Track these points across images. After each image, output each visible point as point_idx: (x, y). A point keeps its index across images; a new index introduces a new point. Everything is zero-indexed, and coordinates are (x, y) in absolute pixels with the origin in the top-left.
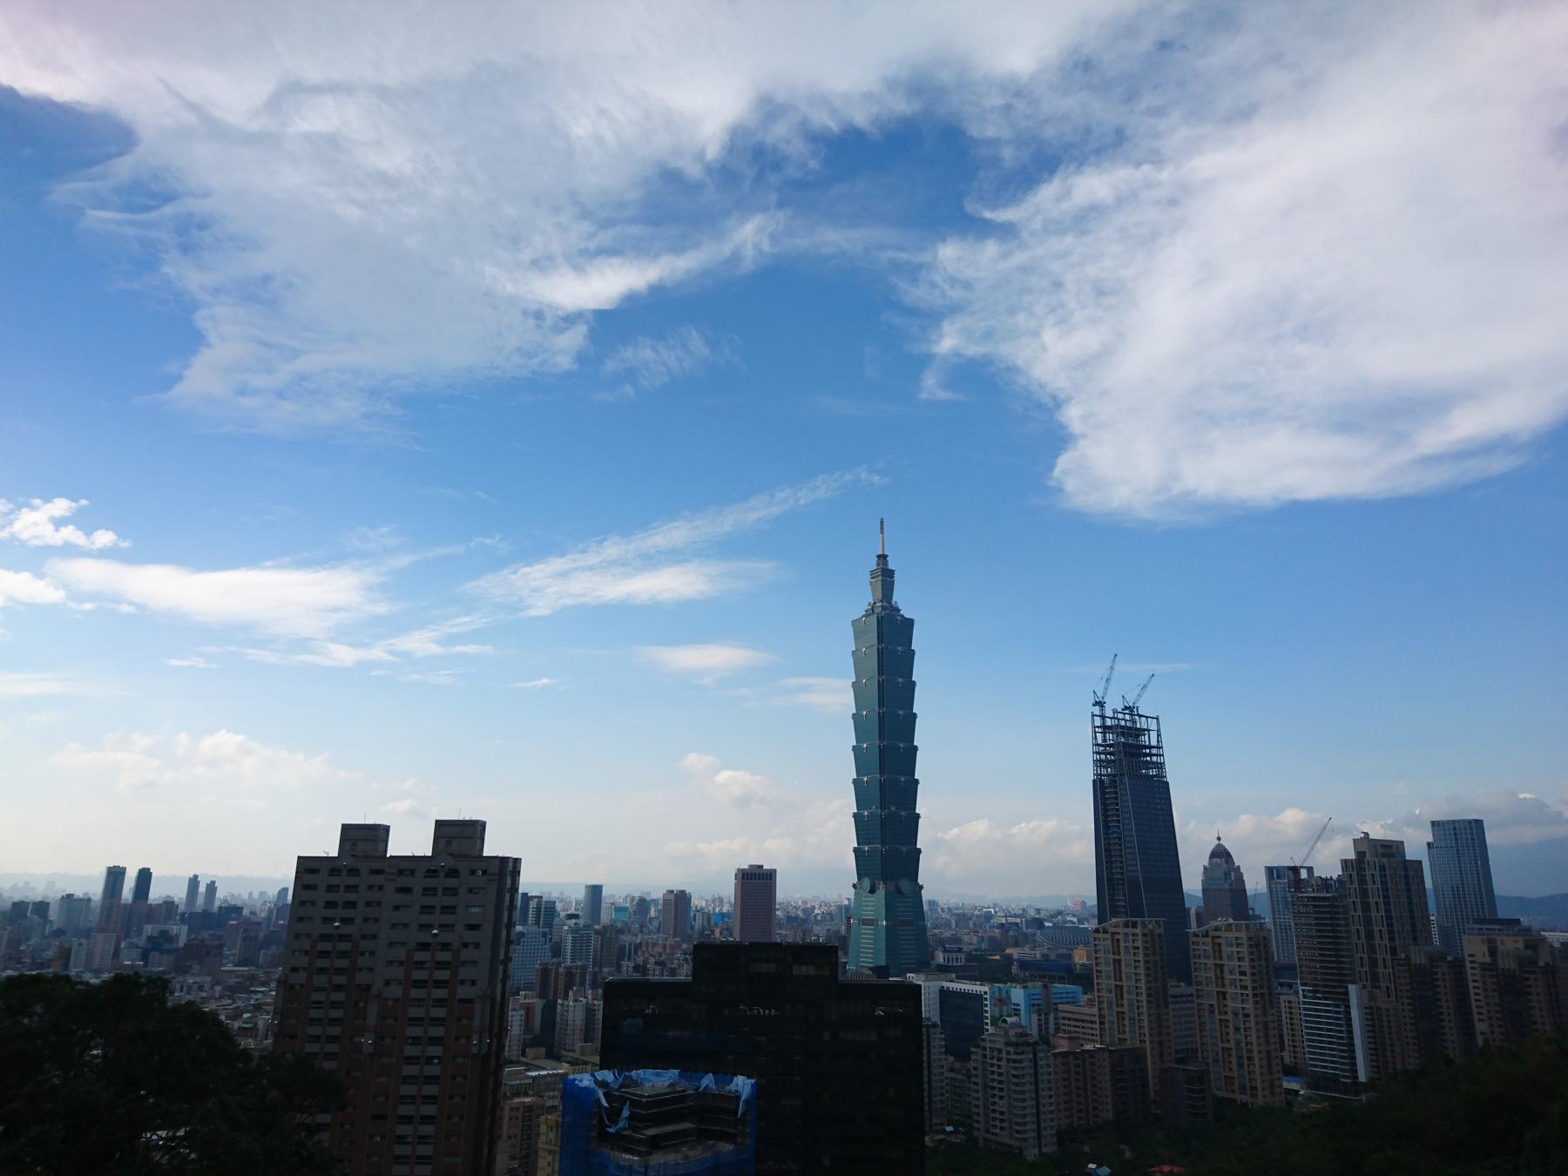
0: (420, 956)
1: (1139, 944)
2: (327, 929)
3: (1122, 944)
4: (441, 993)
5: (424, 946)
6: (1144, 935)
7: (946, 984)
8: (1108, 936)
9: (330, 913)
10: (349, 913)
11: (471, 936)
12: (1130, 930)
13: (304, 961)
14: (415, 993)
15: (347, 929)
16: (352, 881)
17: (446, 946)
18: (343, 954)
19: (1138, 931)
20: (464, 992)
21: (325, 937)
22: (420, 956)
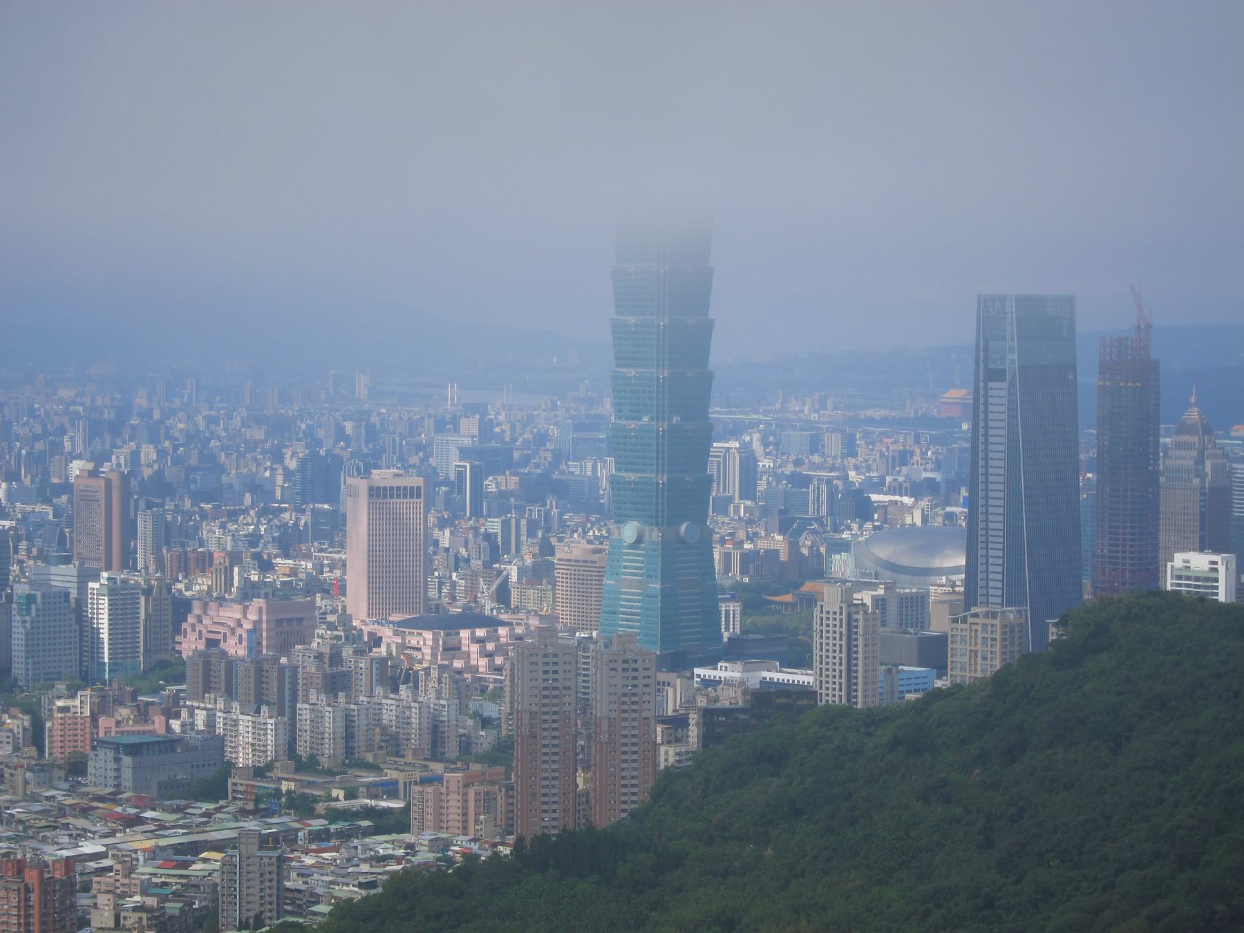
0: (624, 699)
1: (998, 636)
2: (546, 684)
3: (980, 634)
4: (636, 715)
5: (625, 695)
6: (1004, 626)
7: (768, 675)
8: (966, 626)
9: (546, 676)
10: (556, 676)
11: (647, 689)
12: (989, 621)
13: (615, 706)
14: (624, 715)
15: (556, 684)
16: (556, 660)
17: (557, 688)
18: (556, 697)
19: (997, 622)
20: (645, 714)
21: (545, 689)
22: (624, 699)
